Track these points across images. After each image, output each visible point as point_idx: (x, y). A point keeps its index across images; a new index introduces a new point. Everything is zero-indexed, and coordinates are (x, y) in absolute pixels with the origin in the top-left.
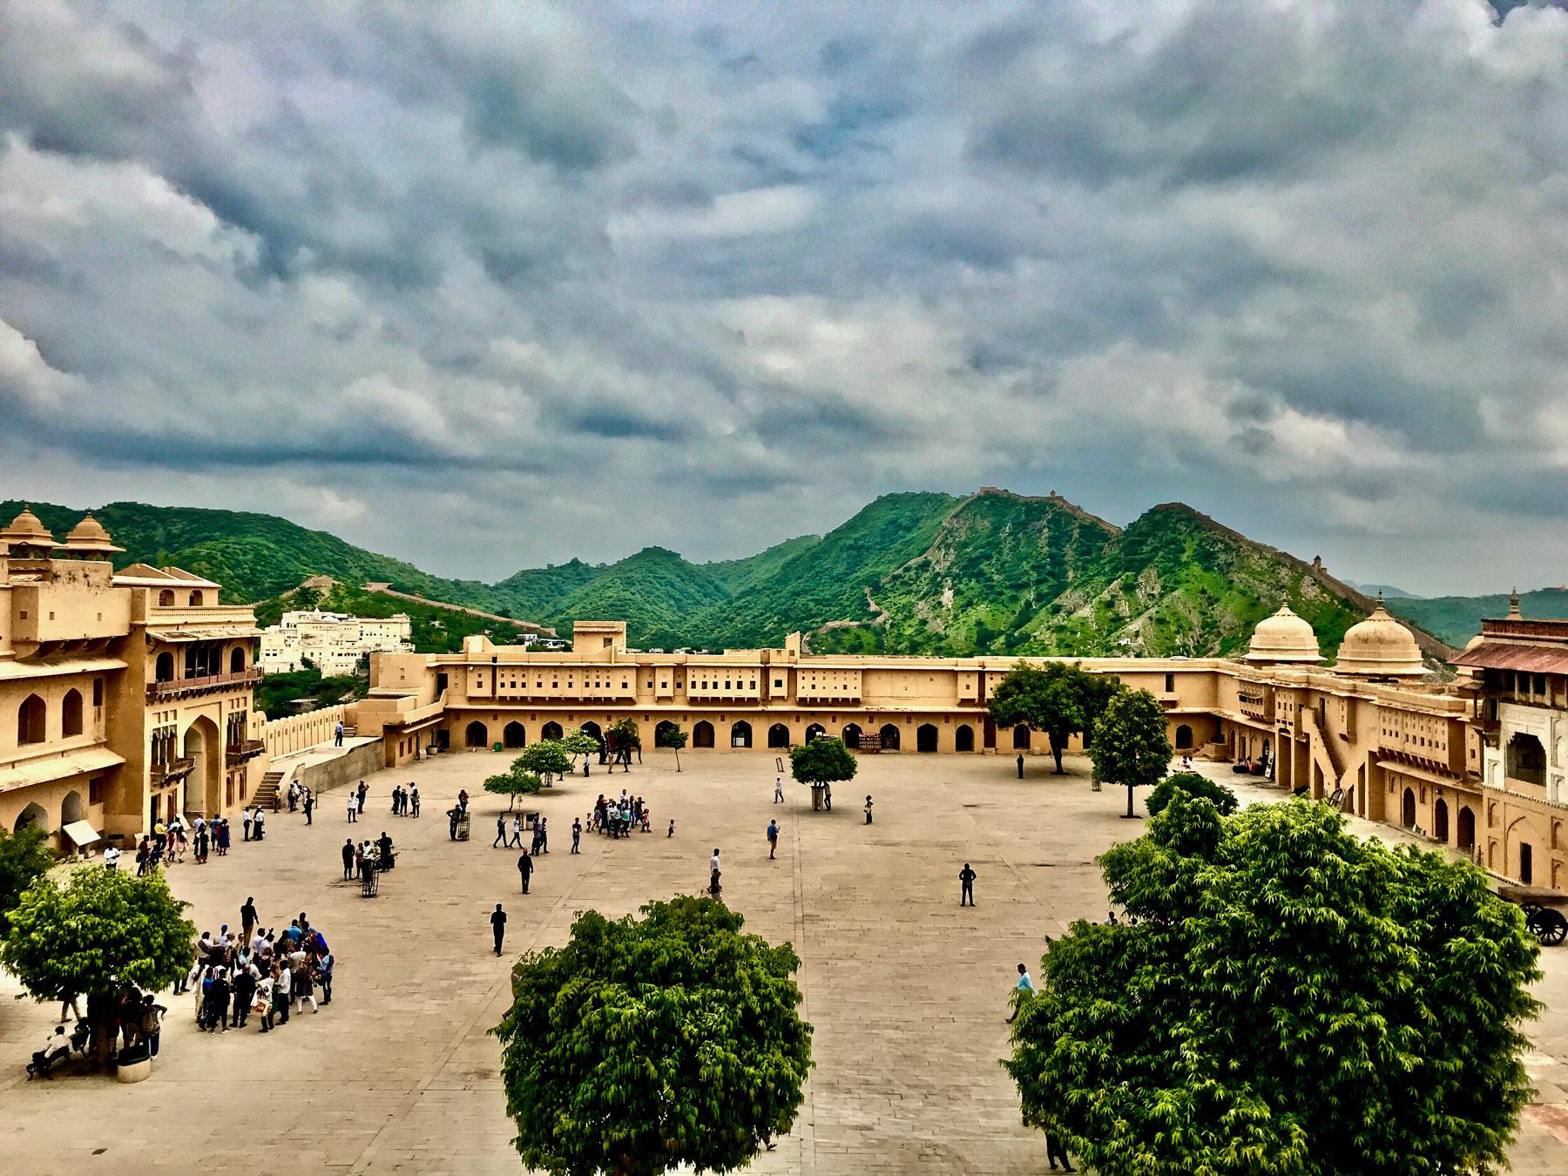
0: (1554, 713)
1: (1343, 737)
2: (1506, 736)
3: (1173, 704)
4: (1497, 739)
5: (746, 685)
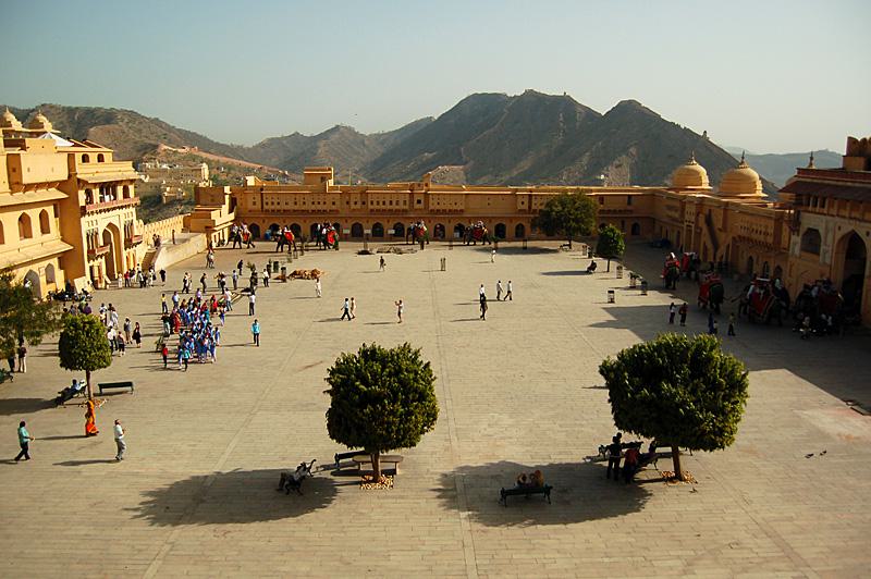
0: (829, 218)
1: (720, 230)
2: (803, 230)
3: (631, 211)
4: (798, 231)
5: (401, 203)
